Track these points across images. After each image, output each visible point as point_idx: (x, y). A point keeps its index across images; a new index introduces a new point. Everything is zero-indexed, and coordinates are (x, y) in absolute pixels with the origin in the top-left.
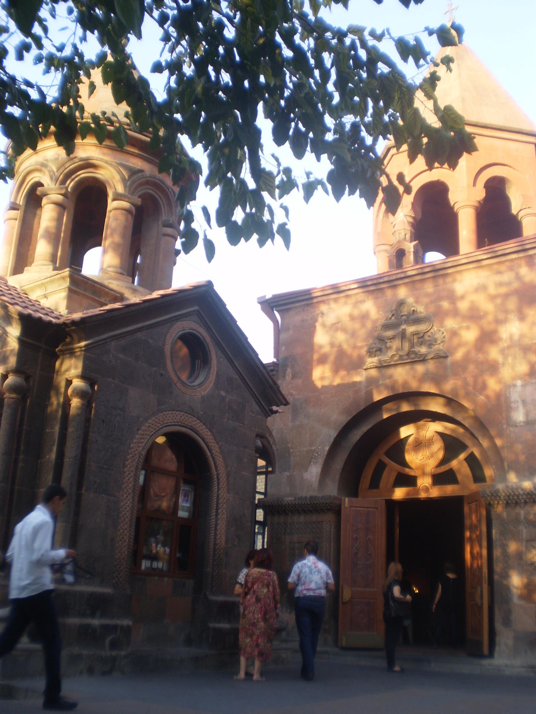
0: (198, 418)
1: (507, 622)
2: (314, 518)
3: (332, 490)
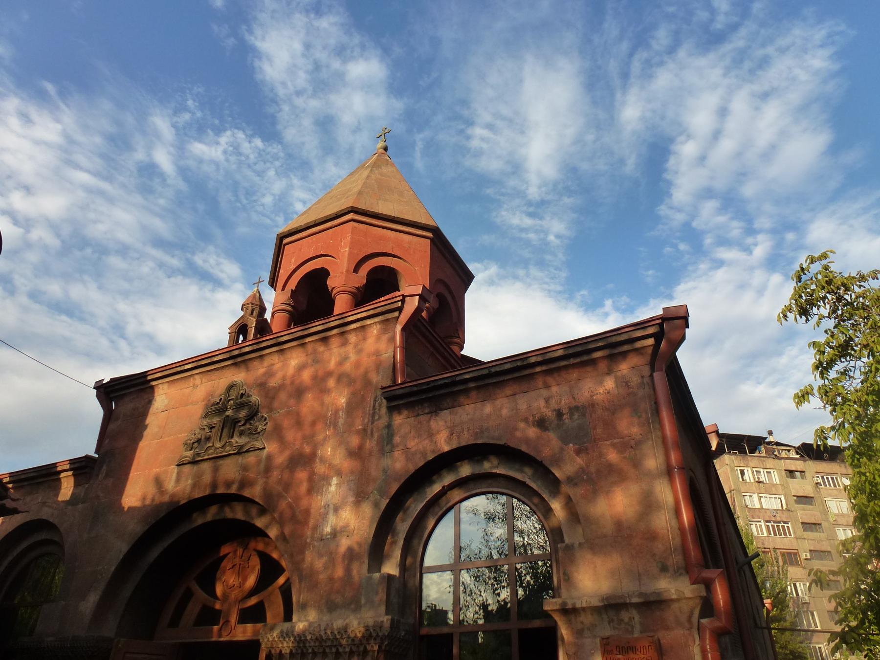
3: (109, 629)
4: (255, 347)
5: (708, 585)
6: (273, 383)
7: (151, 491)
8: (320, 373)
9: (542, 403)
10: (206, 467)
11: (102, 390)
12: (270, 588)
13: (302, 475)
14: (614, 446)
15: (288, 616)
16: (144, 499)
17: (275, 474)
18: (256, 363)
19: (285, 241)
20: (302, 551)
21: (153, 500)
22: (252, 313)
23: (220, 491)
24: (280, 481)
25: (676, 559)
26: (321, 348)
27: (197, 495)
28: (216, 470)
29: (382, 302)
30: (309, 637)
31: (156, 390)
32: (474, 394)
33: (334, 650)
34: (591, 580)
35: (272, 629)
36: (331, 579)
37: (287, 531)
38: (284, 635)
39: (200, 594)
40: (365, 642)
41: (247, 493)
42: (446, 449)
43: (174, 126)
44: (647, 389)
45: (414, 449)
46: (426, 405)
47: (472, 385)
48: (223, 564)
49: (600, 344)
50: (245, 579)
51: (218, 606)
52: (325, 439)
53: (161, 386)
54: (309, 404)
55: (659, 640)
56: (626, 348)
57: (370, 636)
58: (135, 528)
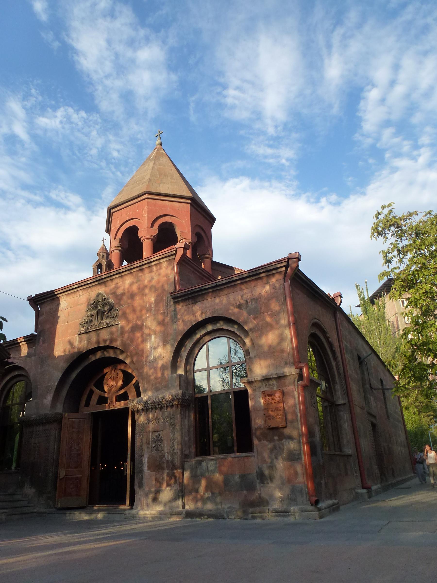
1: (141, 486)
2: (47, 427)
3: (59, 409)
4: (107, 275)
5: (301, 369)
6: (119, 292)
7: (68, 347)
8: (141, 286)
9: (240, 297)
10: (93, 335)
11: (32, 300)
12: (130, 385)
13: (138, 335)
14: (269, 315)
15: (139, 395)
16: (65, 351)
17: (126, 336)
18: (110, 283)
19: (112, 211)
20: (142, 368)
21: (69, 351)
22: (103, 257)
23: (102, 344)
25: (291, 360)
26: (140, 274)
27: (91, 347)
28: (98, 335)
29: (166, 251)
30: (149, 402)
31: (60, 299)
32: (210, 294)
33: (160, 406)
34: (260, 369)
35: (133, 401)
36: (156, 378)
37: (135, 360)
39: (97, 392)
40: (172, 401)
41: (114, 345)
42: (200, 319)
43: (24, 108)
44: (282, 290)
45: (187, 320)
46: (190, 300)
47: (210, 290)
48: (106, 377)
50: (117, 382)
51: (106, 396)
52: (147, 318)
53: (62, 297)
54: (138, 301)
55: (283, 391)
56: (274, 272)
57: (174, 399)
58: (64, 366)
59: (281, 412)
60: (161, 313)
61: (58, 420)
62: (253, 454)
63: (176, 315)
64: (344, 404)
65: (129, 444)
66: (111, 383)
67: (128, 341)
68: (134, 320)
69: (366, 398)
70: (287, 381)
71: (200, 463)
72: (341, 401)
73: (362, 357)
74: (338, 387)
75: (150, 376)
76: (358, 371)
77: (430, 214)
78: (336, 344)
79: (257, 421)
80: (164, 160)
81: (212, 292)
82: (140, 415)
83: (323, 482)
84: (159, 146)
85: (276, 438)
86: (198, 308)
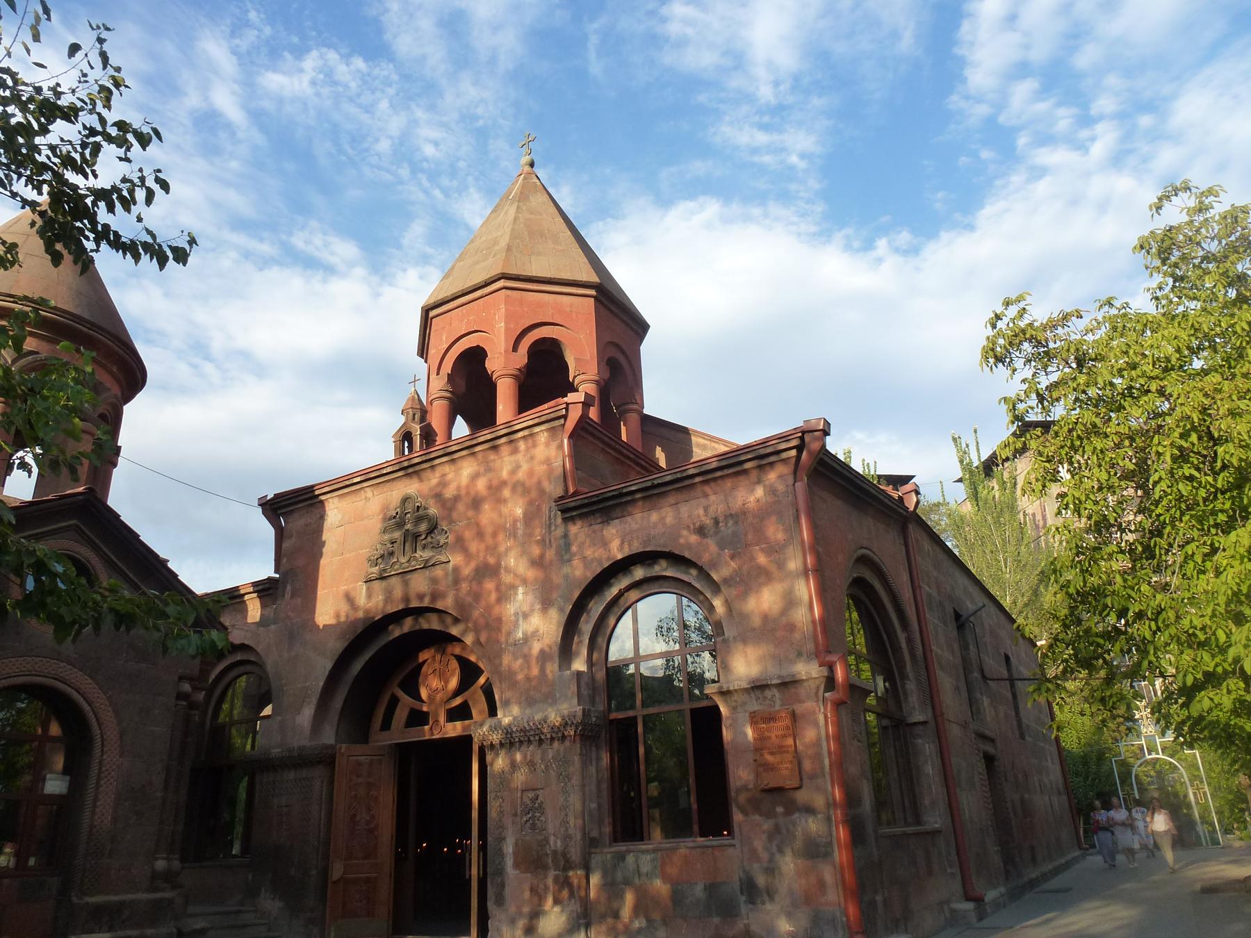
0: (69, 663)
1: (500, 901)
3: (328, 737)
4: (424, 458)
6: (449, 493)
7: (344, 608)
8: (495, 482)
9: (701, 512)
13: (489, 585)
14: (762, 550)
15: (493, 712)
16: (338, 616)
17: (464, 586)
18: (428, 474)
19: (432, 314)
20: (499, 655)
21: (347, 616)
24: (469, 593)
25: (810, 646)
26: (492, 456)
27: (391, 609)
28: (406, 584)
32: (640, 503)
34: (745, 665)
35: (481, 725)
36: (528, 679)
37: (483, 639)
38: (493, 729)
41: (439, 605)
42: (620, 557)
47: (638, 496)
48: (424, 669)
49: (749, 456)
50: (447, 682)
51: (425, 709)
52: (508, 550)
54: (487, 515)
58: (336, 646)
59: (789, 757)
60: (538, 542)
61: (327, 759)
62: (732, 842)
63: (568, 546)
64: (925, 723)
65: (475, 814)
66: (435, 683)
67: (469, 599)
68: (482, 554)
69: (972, 702)
70: (802, 691)
71: (621, 857)
72: (918, 717)
73: (964, 614)
74: (911, 686)
75: (515, 673)
76: (956, 646)
77: (1111, 305)
78: (906, 594)
79: (740, 775)
80: (539, 200)
81: (643, 498)
82: (497, 755)
83: (879, 898)
84: (527, 168)
85: (780, 809)
86: (614, 531)
